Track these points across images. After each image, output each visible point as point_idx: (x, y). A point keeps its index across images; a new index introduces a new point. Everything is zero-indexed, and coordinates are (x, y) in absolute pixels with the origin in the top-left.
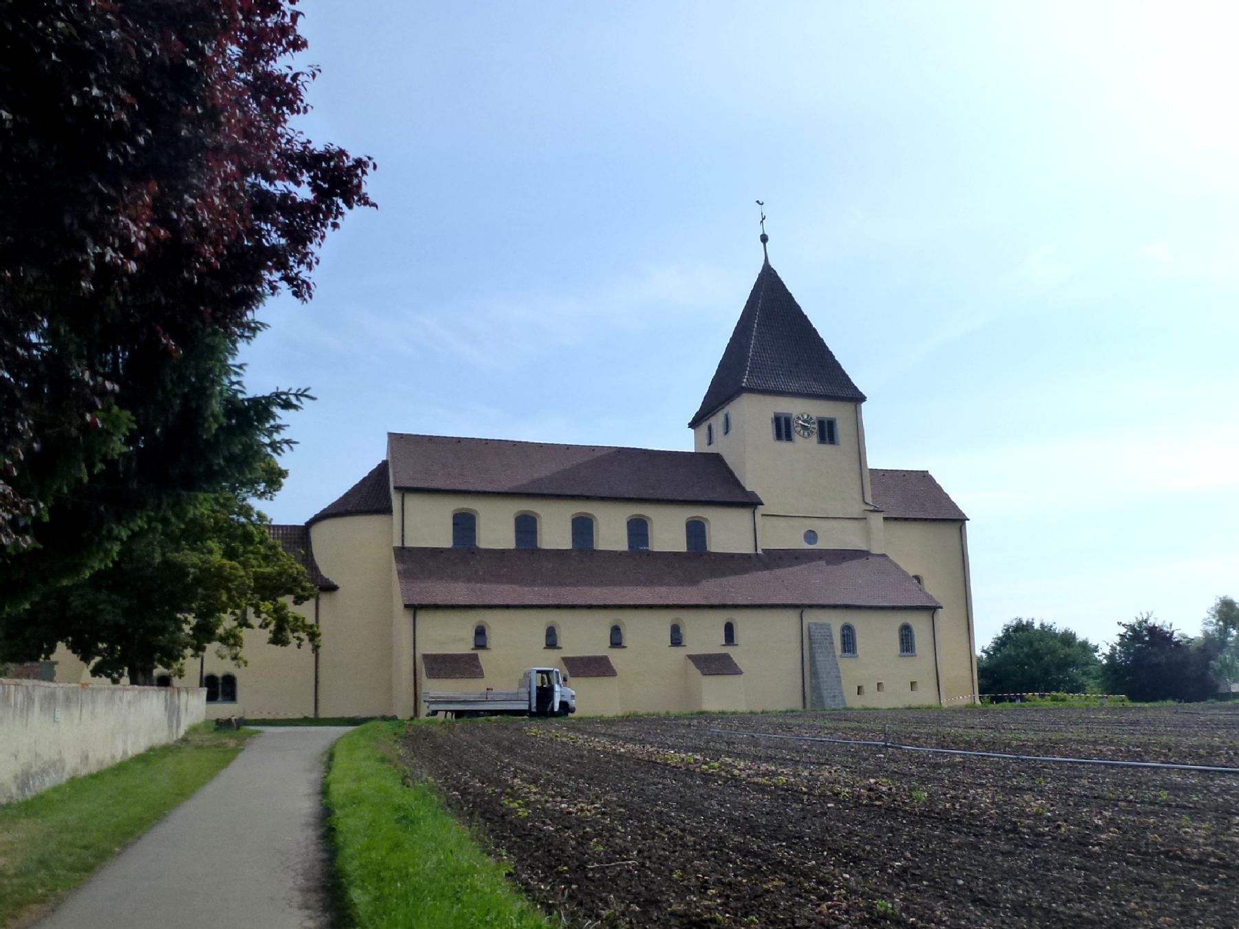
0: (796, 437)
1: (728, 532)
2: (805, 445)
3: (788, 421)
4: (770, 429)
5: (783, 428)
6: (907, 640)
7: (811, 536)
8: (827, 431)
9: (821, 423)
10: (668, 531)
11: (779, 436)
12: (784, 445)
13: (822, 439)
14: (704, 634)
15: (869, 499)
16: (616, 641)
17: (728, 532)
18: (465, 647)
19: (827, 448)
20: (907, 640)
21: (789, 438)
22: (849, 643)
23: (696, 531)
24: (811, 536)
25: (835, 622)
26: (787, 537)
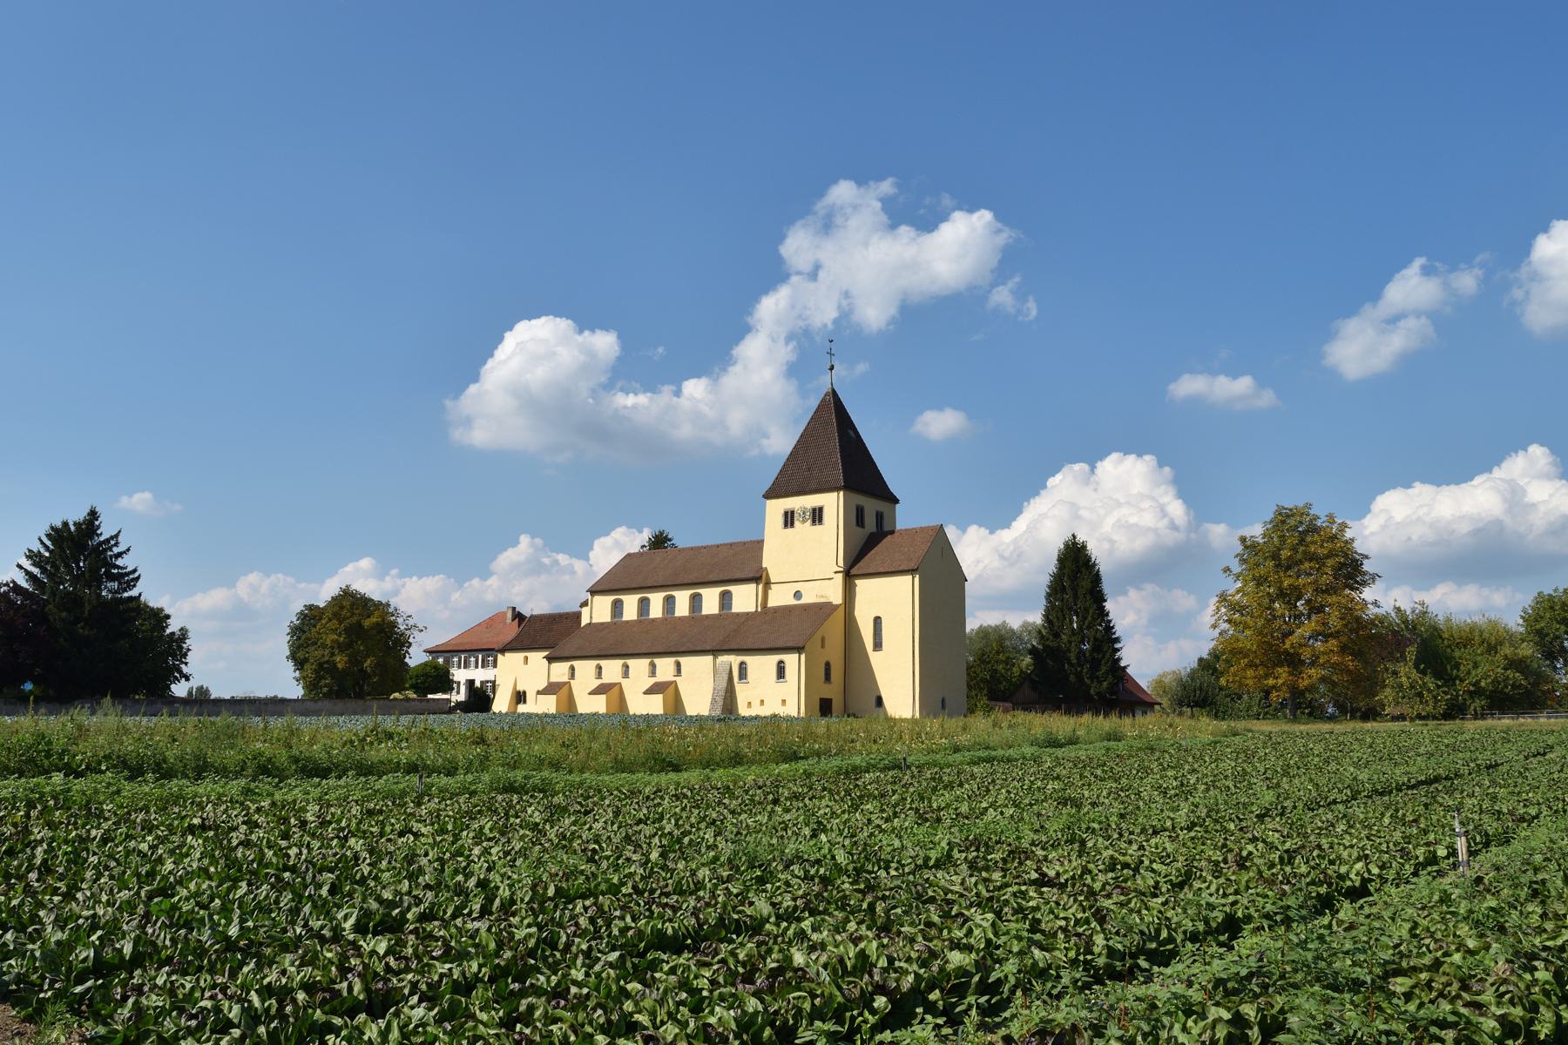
0: (797, 523)
1: (745, 599)
2: (803, 528)
4: (781, 520)
5: (789, 519)
6: (781, 672)
7: (798, 595)
8: (817, 515)
9: (814, 510)
10: (711, 600)
11: (786, 525)
12: (789, 530)
13: (814, 522)
14: (665, 667)
15: (841, 563)
16: (626, 674)
17: (745, 599)
18: (565, 679)
19: (818, 527)
20: (781, 672)
21: (792, 525)
22: (743, 673)
24: (798, 595)
25: (734, 660)
26: (780, 597)
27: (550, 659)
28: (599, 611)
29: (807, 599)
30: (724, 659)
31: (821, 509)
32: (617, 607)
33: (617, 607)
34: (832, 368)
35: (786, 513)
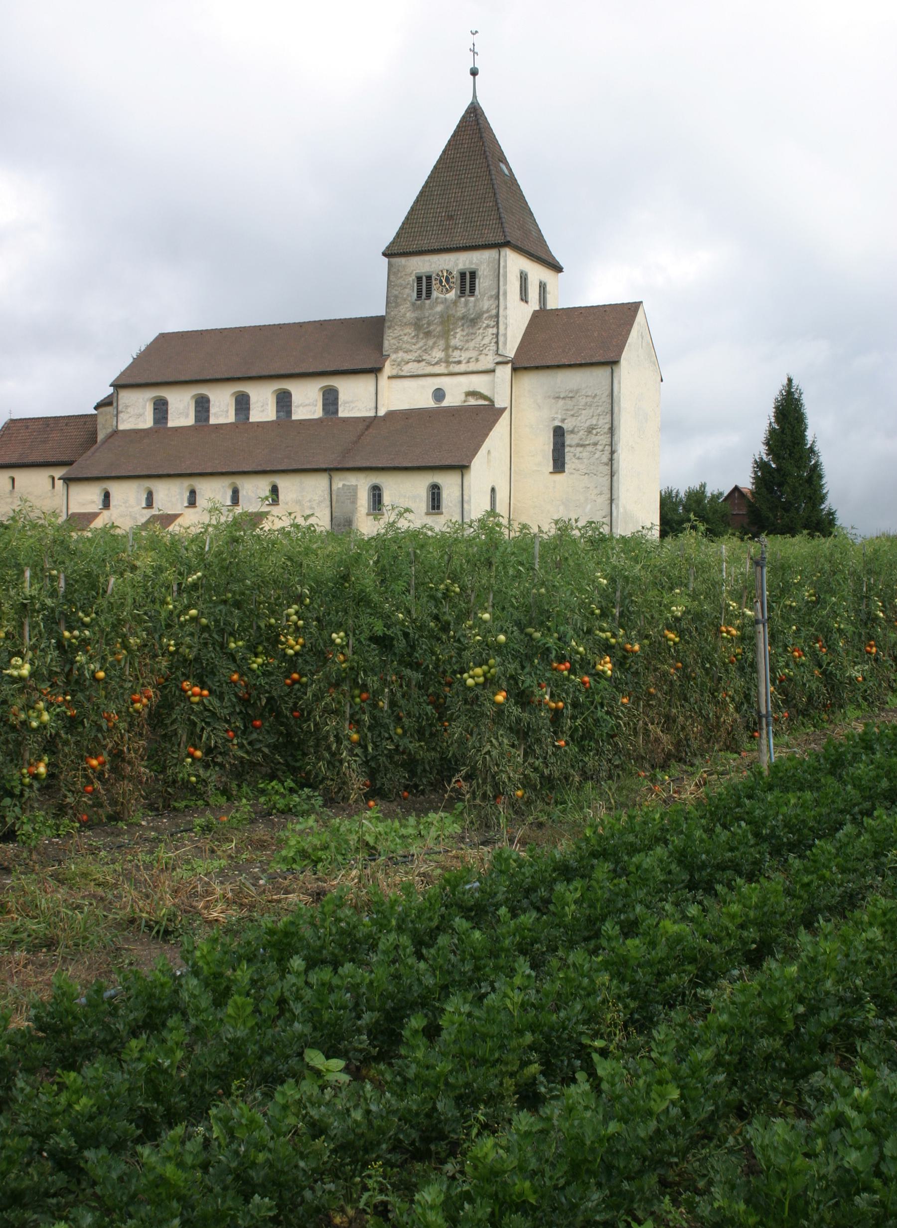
1: (357, 398)
3: (429, 278)
7: (439, 394)
8: (467, 282)
9: (463, 275)
10: (307, 401)
17: (357, 398)
23: (330, 399)
24: (439, 394)
27: (68, 480)
28: (137, 412)
29: (454, 399)
30: (341, 481)
31: (473, 275)
32: (161, 408)
33: (161, 408)
34: (474, 73)
35: (419, 279)
